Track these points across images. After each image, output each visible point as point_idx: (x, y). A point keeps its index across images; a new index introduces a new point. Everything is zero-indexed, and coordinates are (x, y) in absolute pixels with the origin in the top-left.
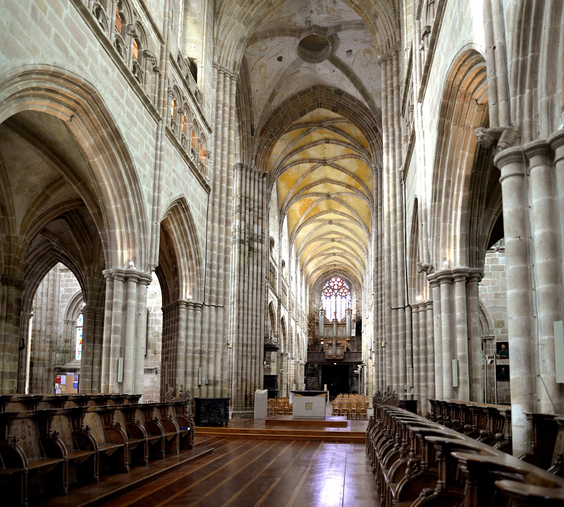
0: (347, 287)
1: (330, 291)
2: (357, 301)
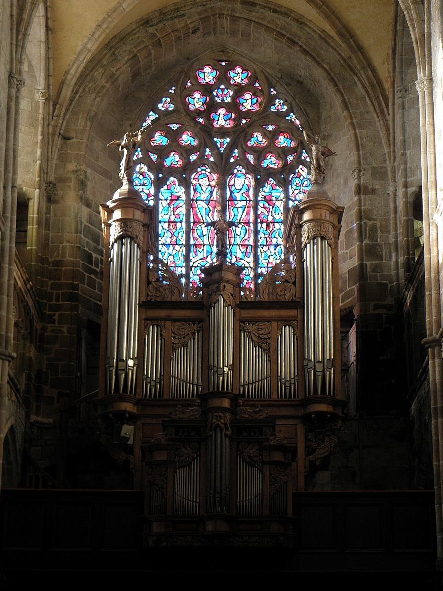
1: (187, 139)
2: (360, 190)
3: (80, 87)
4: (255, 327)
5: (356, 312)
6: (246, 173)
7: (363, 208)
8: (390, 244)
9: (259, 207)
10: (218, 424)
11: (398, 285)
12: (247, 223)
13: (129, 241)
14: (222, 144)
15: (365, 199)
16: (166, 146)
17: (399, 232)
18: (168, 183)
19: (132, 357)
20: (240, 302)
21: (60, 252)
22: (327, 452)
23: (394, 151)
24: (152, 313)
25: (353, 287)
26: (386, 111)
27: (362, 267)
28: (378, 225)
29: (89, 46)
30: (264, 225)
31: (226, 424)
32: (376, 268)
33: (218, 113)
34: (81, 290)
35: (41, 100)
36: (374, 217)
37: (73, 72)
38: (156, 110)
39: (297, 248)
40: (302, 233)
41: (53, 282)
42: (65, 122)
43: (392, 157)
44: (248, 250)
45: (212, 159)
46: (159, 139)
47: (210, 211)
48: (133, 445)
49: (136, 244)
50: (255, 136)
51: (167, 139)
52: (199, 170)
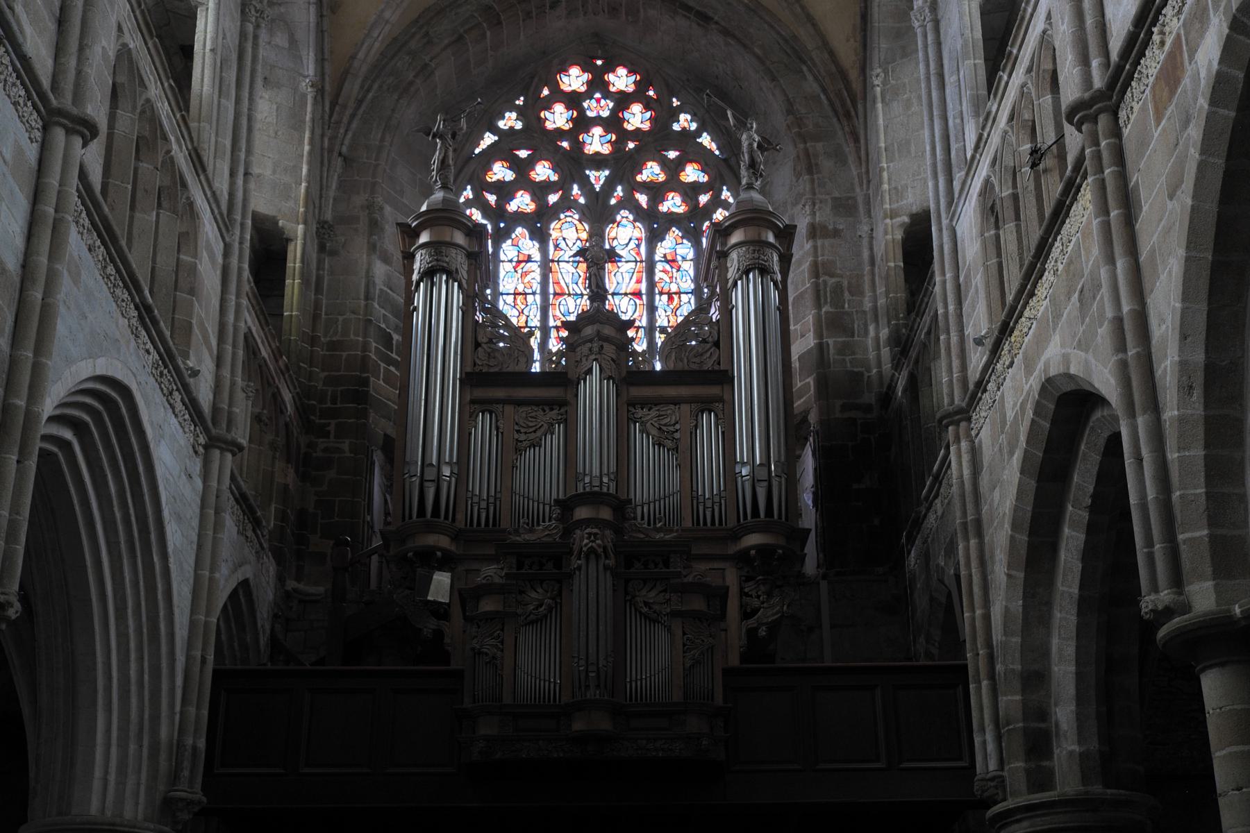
0: (705, 140)
1: (543, 172)
3: (374, 81)
4: (653, 413)
5: (813, 418)
6: (635, 220)
7: (820, 259)
8: (864, 312)
9: (657, 271)
10: (592, 547)
11: (880, 373)
12: (637, 294)
13: (444, 277)
14: (598, 179)
15: (823, 246)
16: (510, 182)
17: (878, 292)
18: (513, 236)
19: (447, 460)
20: (627, 372)
21: (340, 330)
22: (776, 614)
23: (867, 172)
24: (480, 393)
25: (807, 380)
26: (853, 113)
27: (821, 348)
28: (845, 283)
29: (387, 15)
30: (665, 298)
31: (605, 548)
32: (844, 349)
33: (591, 134)
34: (373, 388)
35: (310, 94)
36: (839, 272)
37: (361, 55)
38: (495, 130)
39: (720, 289)
40: (729, 265)
41: (326, 374)
42: (350, 135)
43: (865, 181)
44: (639, 335)
45: (582, 200)
46: (500, 172)
47: (580, 276)
48: (448, 605)
49: (456, 284)
50: (649, 166)
51: (512, 173)
52: (562, 216)
